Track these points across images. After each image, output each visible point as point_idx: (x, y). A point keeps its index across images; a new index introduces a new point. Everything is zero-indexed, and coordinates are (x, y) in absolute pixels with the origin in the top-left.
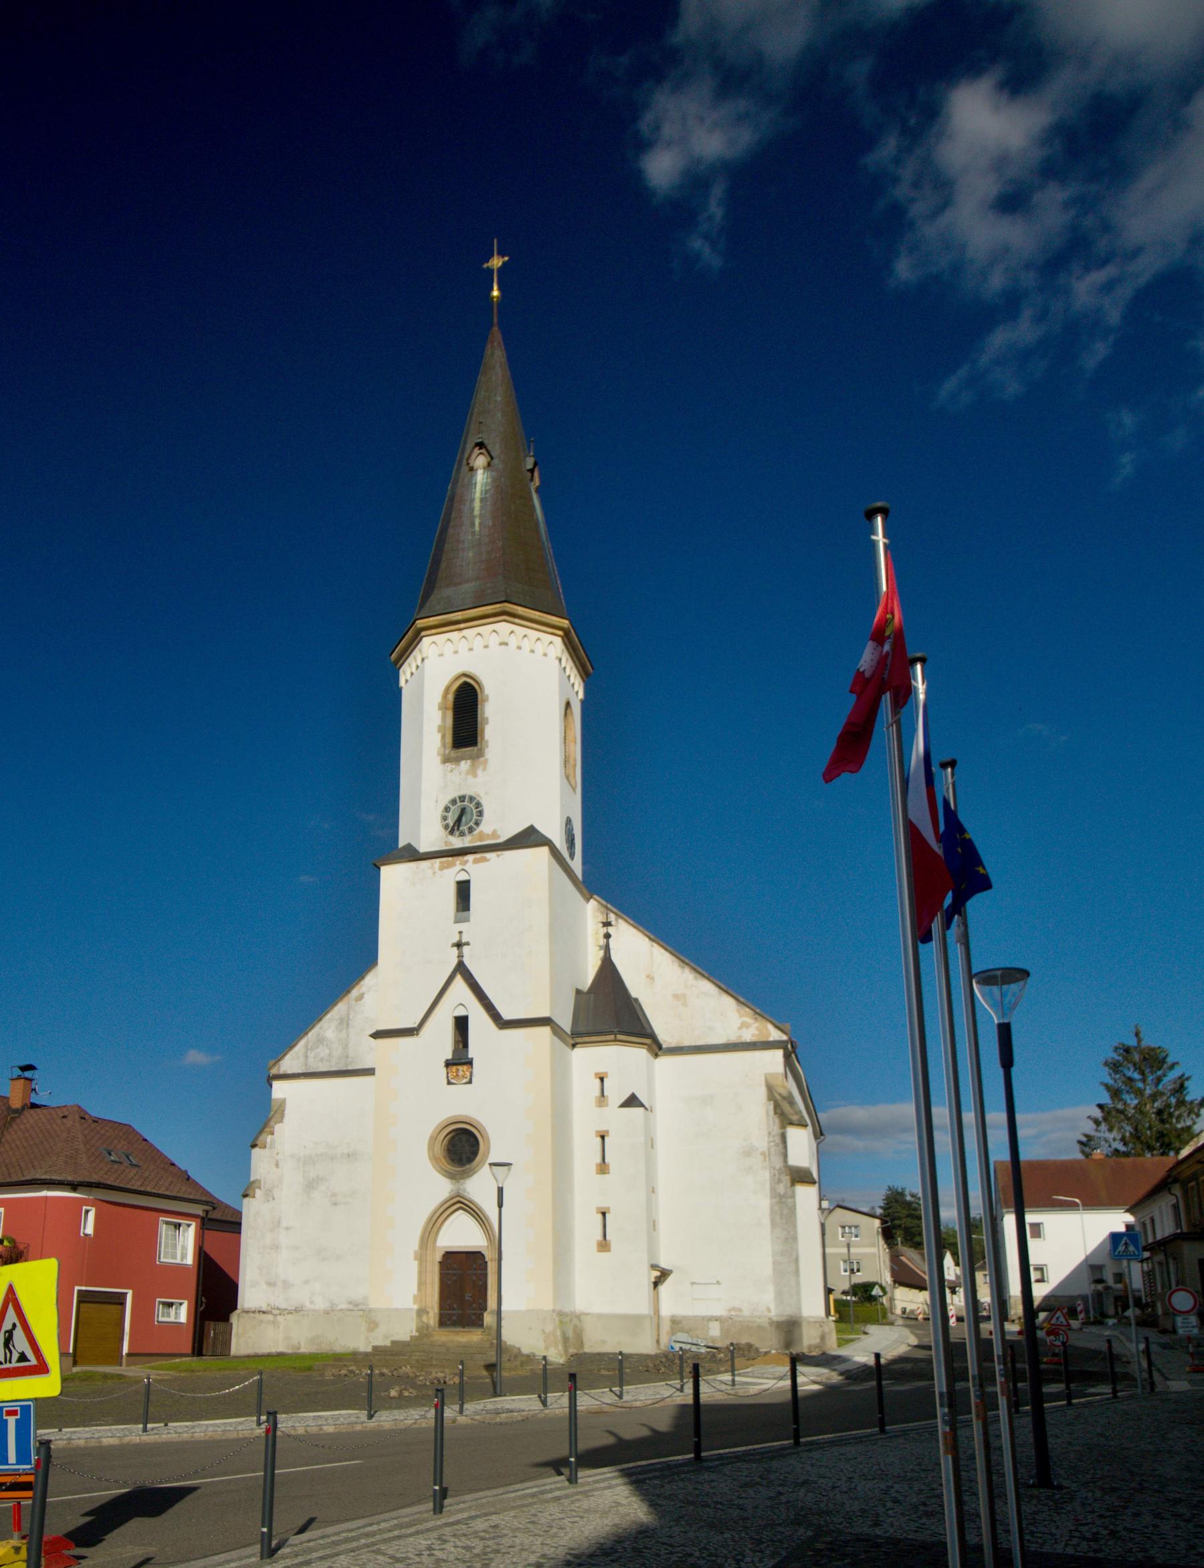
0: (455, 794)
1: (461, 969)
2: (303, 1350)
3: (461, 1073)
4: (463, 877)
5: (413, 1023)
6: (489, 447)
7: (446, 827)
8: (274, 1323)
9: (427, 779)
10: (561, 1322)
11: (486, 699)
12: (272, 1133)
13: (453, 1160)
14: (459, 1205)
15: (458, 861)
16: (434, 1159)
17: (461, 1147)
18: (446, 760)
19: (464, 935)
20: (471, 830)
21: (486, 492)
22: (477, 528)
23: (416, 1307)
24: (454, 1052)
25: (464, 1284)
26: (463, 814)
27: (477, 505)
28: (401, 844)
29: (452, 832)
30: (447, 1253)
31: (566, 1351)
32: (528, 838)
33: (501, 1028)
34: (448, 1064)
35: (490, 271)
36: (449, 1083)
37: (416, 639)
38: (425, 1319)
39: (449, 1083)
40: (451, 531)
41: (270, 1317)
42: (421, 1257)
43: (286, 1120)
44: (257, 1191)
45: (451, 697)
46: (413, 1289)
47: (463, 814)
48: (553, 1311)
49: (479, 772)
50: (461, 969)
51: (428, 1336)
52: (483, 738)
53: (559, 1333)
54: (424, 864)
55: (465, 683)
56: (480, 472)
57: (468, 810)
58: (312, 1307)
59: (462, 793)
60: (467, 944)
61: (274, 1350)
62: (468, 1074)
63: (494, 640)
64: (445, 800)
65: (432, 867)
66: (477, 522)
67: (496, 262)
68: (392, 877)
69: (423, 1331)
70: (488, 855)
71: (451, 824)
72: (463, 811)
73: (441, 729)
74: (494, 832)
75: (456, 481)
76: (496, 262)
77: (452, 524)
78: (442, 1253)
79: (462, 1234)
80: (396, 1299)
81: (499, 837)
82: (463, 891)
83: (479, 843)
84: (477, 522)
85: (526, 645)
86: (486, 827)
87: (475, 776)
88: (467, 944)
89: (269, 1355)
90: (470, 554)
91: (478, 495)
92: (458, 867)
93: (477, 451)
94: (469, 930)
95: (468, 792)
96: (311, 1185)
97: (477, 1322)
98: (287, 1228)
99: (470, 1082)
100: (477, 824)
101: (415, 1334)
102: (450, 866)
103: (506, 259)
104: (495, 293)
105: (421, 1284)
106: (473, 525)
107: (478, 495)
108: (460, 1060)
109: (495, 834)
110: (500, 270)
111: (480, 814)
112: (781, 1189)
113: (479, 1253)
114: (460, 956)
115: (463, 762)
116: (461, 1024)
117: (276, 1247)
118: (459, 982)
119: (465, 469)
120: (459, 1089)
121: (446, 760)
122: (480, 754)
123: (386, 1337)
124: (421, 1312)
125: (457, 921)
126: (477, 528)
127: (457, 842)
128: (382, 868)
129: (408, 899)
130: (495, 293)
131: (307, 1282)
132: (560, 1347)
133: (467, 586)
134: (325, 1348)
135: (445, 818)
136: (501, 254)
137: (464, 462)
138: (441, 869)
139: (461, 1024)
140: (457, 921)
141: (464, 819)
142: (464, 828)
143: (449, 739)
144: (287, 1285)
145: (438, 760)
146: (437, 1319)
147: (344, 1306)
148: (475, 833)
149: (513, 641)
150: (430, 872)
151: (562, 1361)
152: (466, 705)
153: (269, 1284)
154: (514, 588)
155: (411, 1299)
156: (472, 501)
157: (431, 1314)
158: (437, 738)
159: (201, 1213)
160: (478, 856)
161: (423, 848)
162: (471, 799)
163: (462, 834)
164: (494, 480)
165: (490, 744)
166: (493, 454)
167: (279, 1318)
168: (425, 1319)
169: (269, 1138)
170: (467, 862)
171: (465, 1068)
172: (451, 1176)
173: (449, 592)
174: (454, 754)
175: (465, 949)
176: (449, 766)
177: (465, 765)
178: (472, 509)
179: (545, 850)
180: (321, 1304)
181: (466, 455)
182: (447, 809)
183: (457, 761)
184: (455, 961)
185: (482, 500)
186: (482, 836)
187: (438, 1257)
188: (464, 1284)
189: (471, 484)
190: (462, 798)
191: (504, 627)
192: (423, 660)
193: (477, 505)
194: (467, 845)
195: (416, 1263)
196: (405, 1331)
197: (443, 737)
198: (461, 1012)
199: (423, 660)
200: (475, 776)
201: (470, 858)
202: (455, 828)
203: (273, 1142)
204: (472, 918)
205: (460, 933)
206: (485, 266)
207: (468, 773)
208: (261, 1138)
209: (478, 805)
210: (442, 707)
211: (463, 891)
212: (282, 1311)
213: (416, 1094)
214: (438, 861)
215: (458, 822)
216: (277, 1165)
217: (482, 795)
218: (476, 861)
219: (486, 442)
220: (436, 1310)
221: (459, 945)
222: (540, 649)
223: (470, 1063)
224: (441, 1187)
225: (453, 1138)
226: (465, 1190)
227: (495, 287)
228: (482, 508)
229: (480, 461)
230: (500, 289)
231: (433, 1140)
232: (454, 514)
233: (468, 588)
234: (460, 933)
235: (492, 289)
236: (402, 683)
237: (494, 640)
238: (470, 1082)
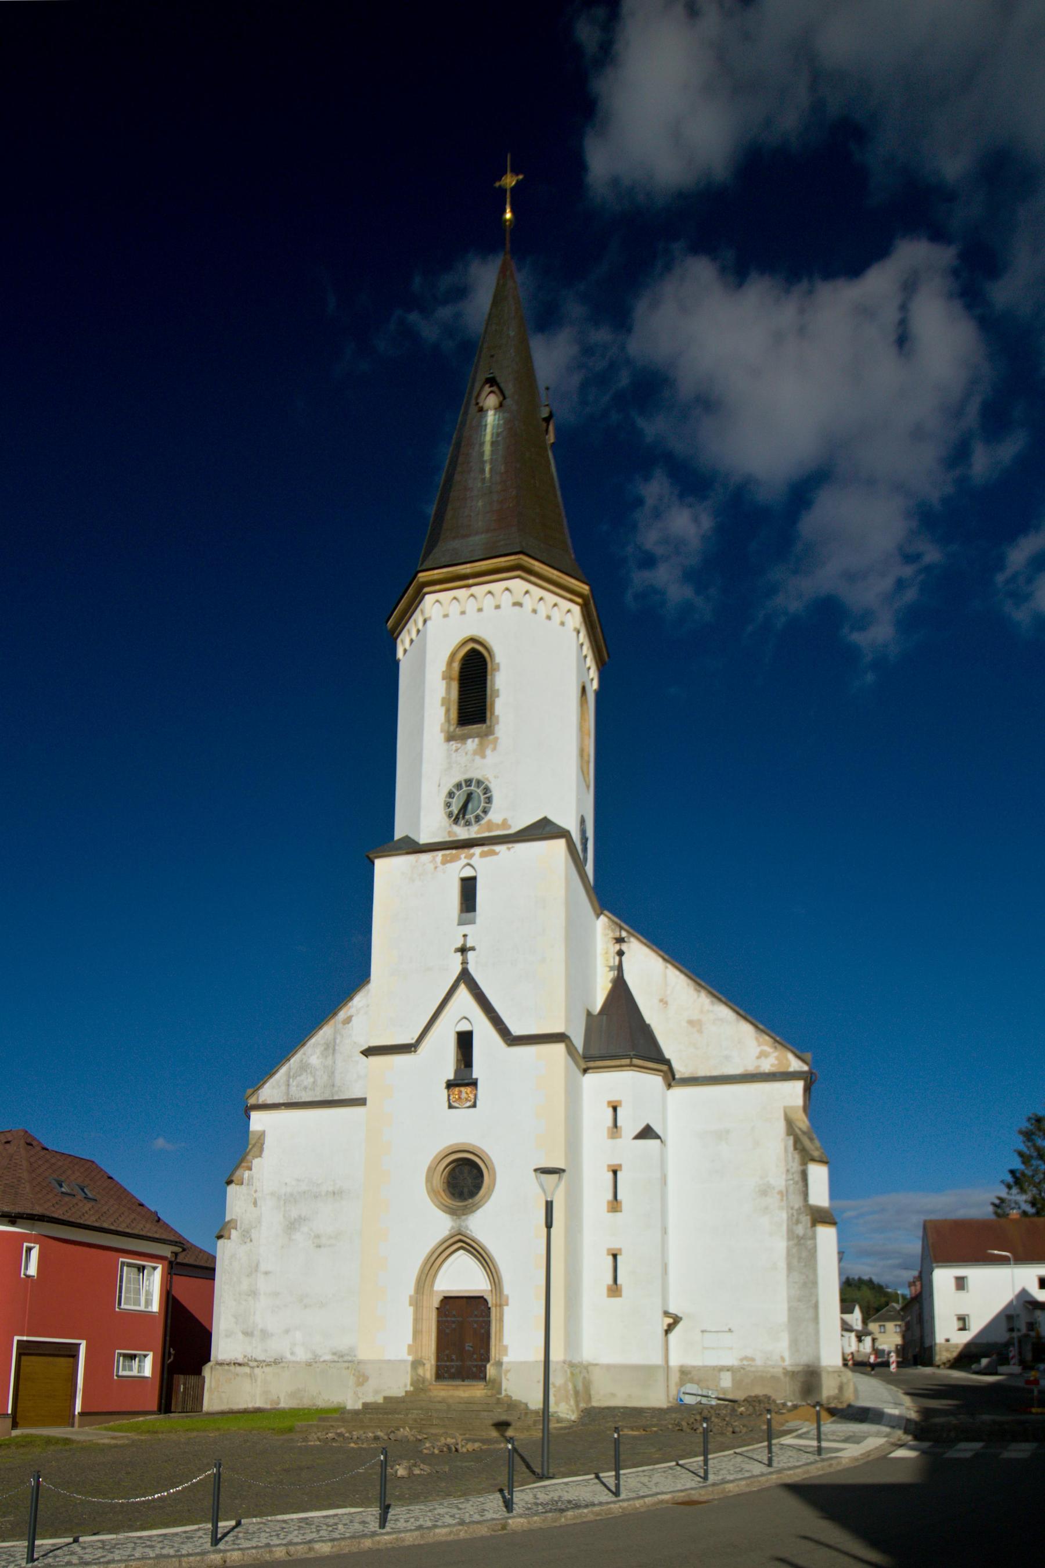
0: (459, 777)
1: (465, 977)
2: (283, 1405)
3: (464, 1095)
4: (468, 873)
5: (409, 1039)
6: (502, 385)
7: (450, 815)
8: (252, 1377)
9: (428, 758)
10: (572, 1374)
11: (497, 668)
12: (250, 1169)
13: (453, 1194)
14: (460, 1244)
15: (463, 853)
16: (432, 1192)
17: (463, 1179)
18: (450, 738)
19: (469, 939)
20: (478, 819)
21: (498, 435)
22: (487, 475)
23: (410, 1358)
24: (456, 1072)
25: (463, 1331)
26: (469, 800)
27: (487, 448)
28: (398, 836)
29: (456, 821)
30: (446, 1298)
31: (577, 1403)
32: (543, 830)
33: (510, 1045)
34: (450, 1085)
35: (502, 191)
36: (450, 1107)
37: (418, 598)
38: (420, 1371)
39: (450, 1107)
40: (457, 477)
41: (247, 1370)
42: (417, 1302)
43: (265, 1153)
44: (233, 1232)
45: (456, 666)
46: (407, 1336)
47: (469, 800)
48: (564, 1362)
49: (488, 752)
51: (423, 1390)
52: (492, 713)
53: (570, 1386)
54: (425, 857)
55: (473, 651)
56: (491, 413)
57: (475, 795)
58: (293, 1358)
59: (467, 776)
60: (473, 949)
61: (251, 1405)
62: (472, 1096)
63: (506, 599)
64: (449, 784)
65: (434, 860)
66: (487, 468)
67: (510, 181)
68: (387, 870)
69: (418, 1384)
70: (497, 848)
71: (456, 812)
72: (469, 797)
73: (445, 702)
74: (505, 821)
75: (463, 423)
76: (510, 181)
77: (459, 469)
78: (440, 1298)
79: (462, 1277)
80: (389, 1349)
81: (510, 827)
82: (468, 888)
83: (486, 834)
84: (487, 468)
85: (542, 609)
86: (495, 815)
87: (483, 756)
88: (473, 949)
89: (245, 1412)
90: (480, 504)
91: (488, 438)
92: (463, 861)
93: (487, 389)
94: (474, 933)
96: (292, 1226)
97: (480, 1374)
98: (266, 1273)
99: (474, 1106)
100: (485, 812)
101: (410, 1388)
102: (454, 859)
103: (521, 177)
104: (508, 216)
105: (417, 1333)
106: (483, 471)
107: (488, 438)
108: (463, 1079)
109: (505, 824)
110: (513, 189)
111: (489, 800)
113: (482, 1297)
114: (465, 962)
115: (470, 741)
116: (465, 1041)
117: (253, 1293)
118: (463, 991)
119: (473, 409)
121: (450, 738)
122: (490, 732)
123: (376, 1392)
124: (416, 1364)
125: (461, 923)
126: (487, 475)
127: (462, 833)
128: (378, 863)
129: (404, 895)
130: (508, 216)
131: (287, 1331)
132: (572, 1402)
133: (477, 538)
134: (306, 1403)
135: (448, 805)
136: (515, 171)
137: (473, 402)
138: (444, 862)
139: (465, 1041)
140: (461, 923)
141: (470, 806)
142: (470, 816)
143: (454, 714)
144: (265, 1334)
145: (441, 737)
146: (434, 1371)
147: (328, 1357)
148: (483, 822)
149: (528, 603)
150: (432, 866)
151: (574, 1417)
152: (473, 673)
153: (248, 1334)
155: (405, 1349)
156: (482, 444)
157: (428, 1366)
158: (441, 711)
159: (169, 1255)
160: (486, 848)
161: (424, 839)
162: (479, 783)
163: (468, 824)
164: (508, 422)
165: (501, 719)
166: (507, 393)
167: (257, 1371)
168: (420, 1371)
169: (247, 1174)
170: (473, 855)
171: (469, 1089)
172: (452, 1212)
173: (456, 544)
174: (459, 731)
175: (470, 955)
176: (454, 745)
177: (472, 744)
178: (482, 454)
179: (561, 843)
180: (302, 1355)
181: (475, 394)
182: (451, 795)
183: (463, 738)
184: (458, 969)
185: (493, 443)
186: (490, 826)
187: (436, 1303)
188: (463, 1331)
189: (481, 426)
190: (469, 782)
191: (518, 585)
192: (425, 621)
193: (487, 448)
194: (474, 836)
195: (411, 1309)
196: (399, 1385)
197: (448, 711)
198: (464, 1027)
199: (425, 621)
200: (483, 756)
201: (477, 851)
202: (460, 816)
203: (251, 1178)
204: (478, 920)
205: (465, 936)
206: (497, 184)
207: (475, 753)
208: (238, 1173)
209: (487, 790)
210: (447, 677)
211: (468, 888)
212: (260, 1363)
213: (412, 1119)
214: (440, 854)
215: (464, 809)
216: (255, 1204)
217: (491, 779)
218: (483, 855)
219: (499, 380)
220: (433, 1362)
221: (463, 950)
222: (556, 615)
223: (474, 1084)
224: (441, 1224)
225: (453, 1169)
226: (467, 1227)
227: (508, 210)
228: (493, 452)
229: (491, 401)
230: (513, 211)
231: (431, 1171)
232: (461, 459)
233: (478, 540)
234: (465, 936)
235: (504, 211)
236: (400, 654)
237: (506, 599)
238: (474, 1106)
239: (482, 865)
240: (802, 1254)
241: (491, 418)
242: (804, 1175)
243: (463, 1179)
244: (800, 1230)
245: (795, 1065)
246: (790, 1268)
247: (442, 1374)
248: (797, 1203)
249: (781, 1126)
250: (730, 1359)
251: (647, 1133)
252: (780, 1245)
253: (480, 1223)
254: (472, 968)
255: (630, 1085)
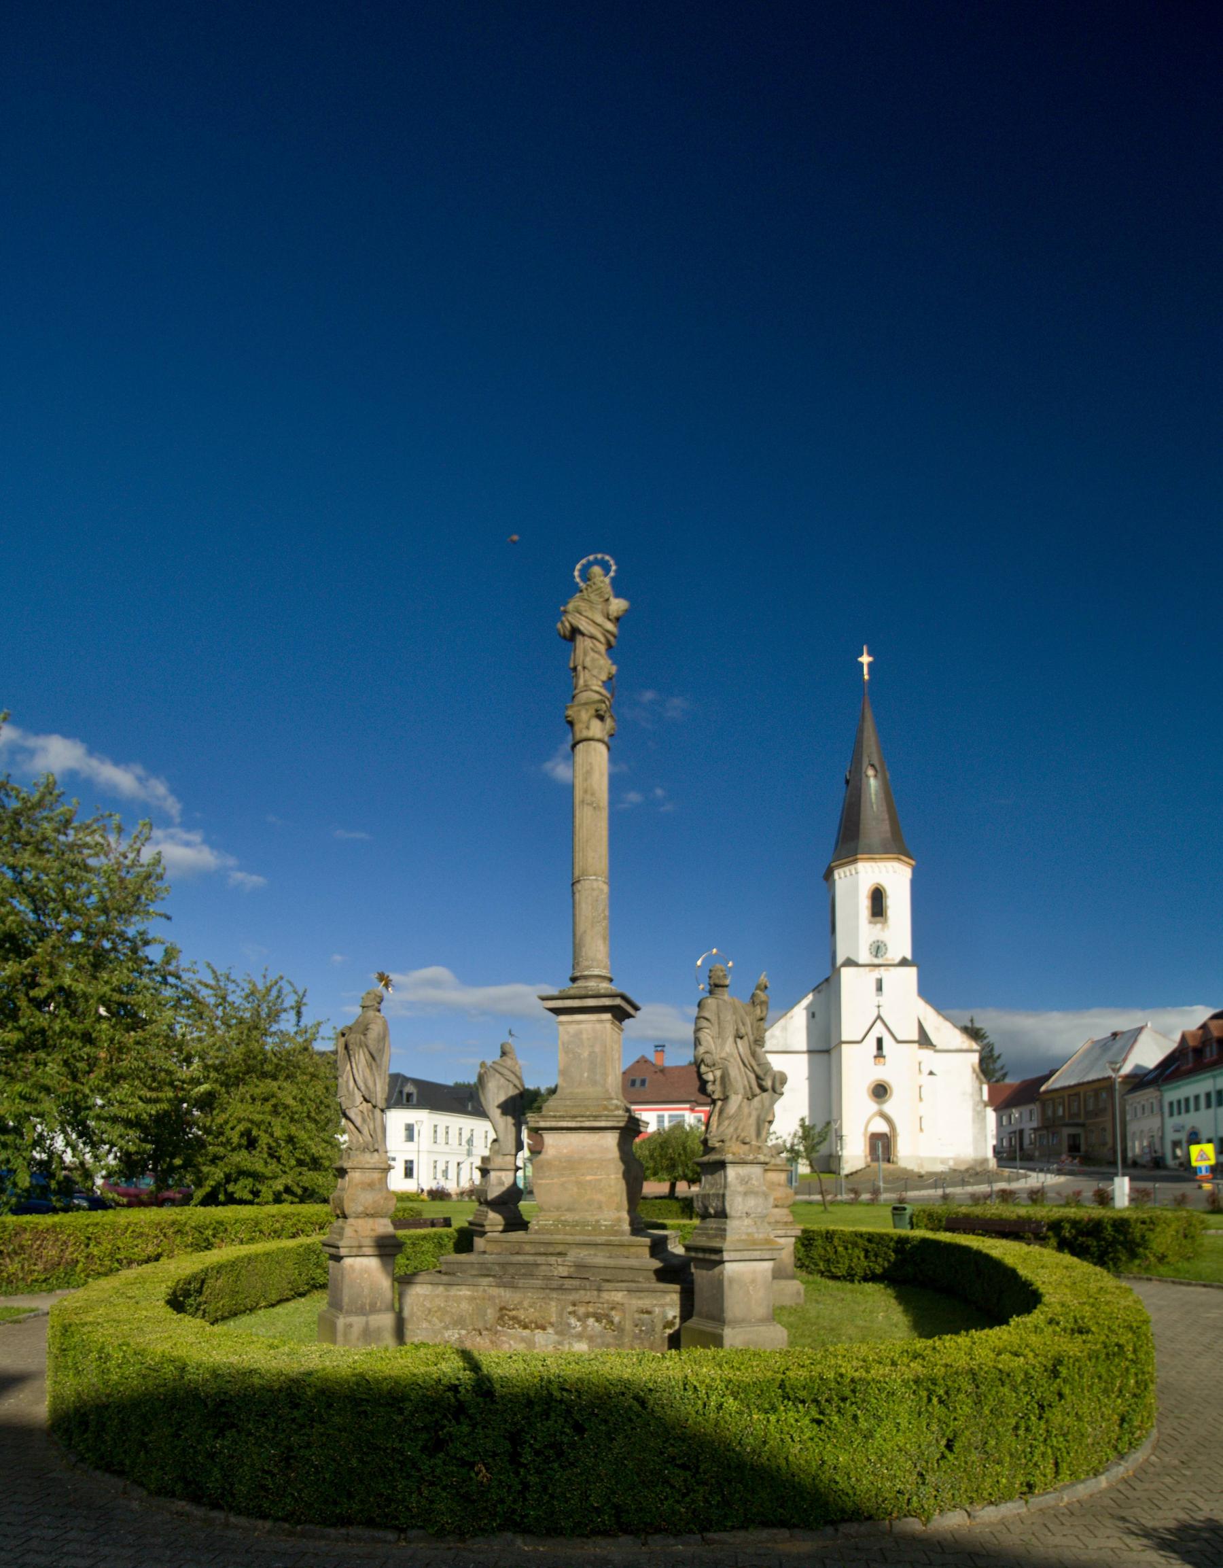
1: (879, 1017)
15: (877, 969)
18: (870, 922)
26: (878, 948)
34: (875, 1057)
42: (865, 1135)
46: (862, 1147)
47: (878, 948)
50: (879, 1017)
79: (881, 1127)
94: (882, 1000)
95: (881, 938)
112: (979, 1108)
116: (880, 1042)
118: (879, 1022)
120: (880, 1068)
121: (870, 922)
122: (886, 921)
127: (876, 961)
139: (880, 1042)
154: (897, 846)
161: (861, 961)
172: (878, 1103)
177: (879, 926)
183: (875, 923)
188: (882, 1145)
224: (873, 1106)
229: (871, 772)
239: (882, 973)
240: (980, 1118)
241: (873, 782)
242: (981, 1089)
243: (880, 1091)
244: (979, 1108)
245: (975, 1046)
246: (974, 1122)
247: (873, 1160)
248: (978, 1098)
249: (970, 1070)
250: (951, 1155)
251: (931, 1073)
252: (969, 1114)
253: (889, 1107)
254: (882, 1015)
255: (926, 1053)
